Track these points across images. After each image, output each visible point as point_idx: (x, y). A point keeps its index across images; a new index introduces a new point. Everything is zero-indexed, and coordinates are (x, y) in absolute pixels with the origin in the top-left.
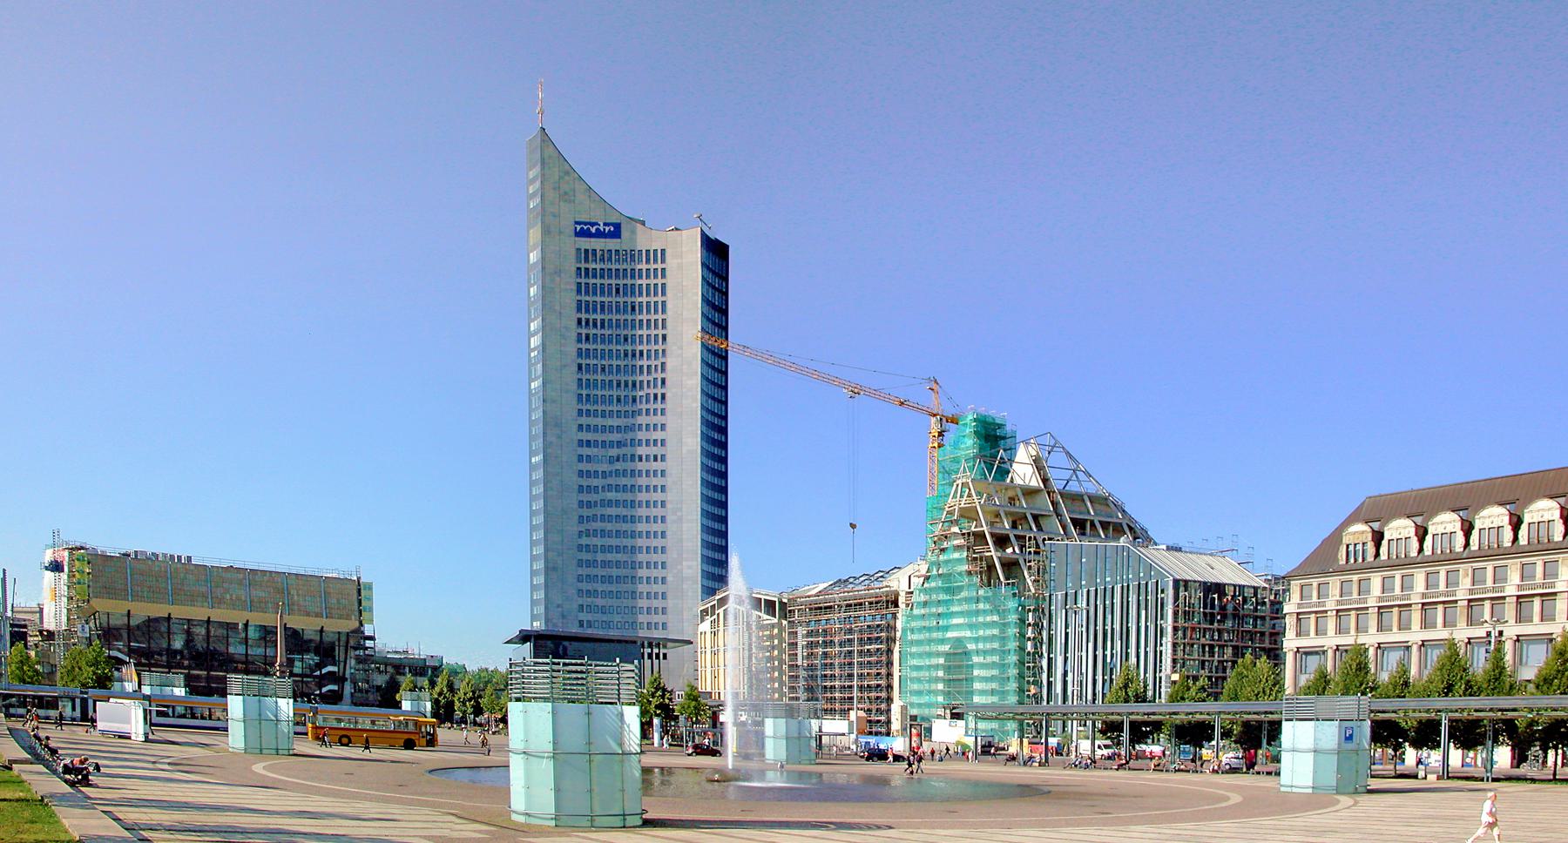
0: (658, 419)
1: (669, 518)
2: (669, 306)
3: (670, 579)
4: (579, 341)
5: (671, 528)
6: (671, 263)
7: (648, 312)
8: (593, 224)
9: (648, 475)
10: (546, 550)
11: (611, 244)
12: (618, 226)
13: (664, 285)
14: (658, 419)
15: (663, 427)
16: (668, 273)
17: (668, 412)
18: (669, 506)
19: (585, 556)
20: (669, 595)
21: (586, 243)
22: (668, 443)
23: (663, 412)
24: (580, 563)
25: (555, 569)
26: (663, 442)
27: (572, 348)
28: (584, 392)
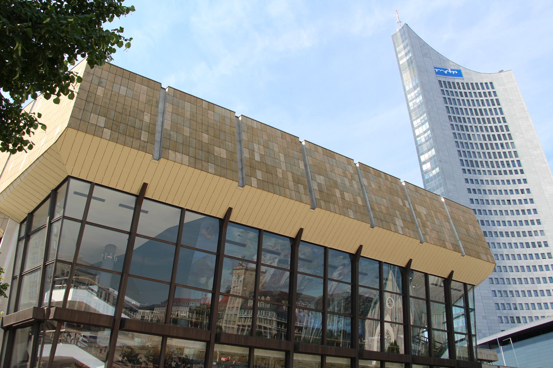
2: (504, 110)
8: (445, 70)
11: (457, 80)
12: (459, 71)
21: (442, 79)
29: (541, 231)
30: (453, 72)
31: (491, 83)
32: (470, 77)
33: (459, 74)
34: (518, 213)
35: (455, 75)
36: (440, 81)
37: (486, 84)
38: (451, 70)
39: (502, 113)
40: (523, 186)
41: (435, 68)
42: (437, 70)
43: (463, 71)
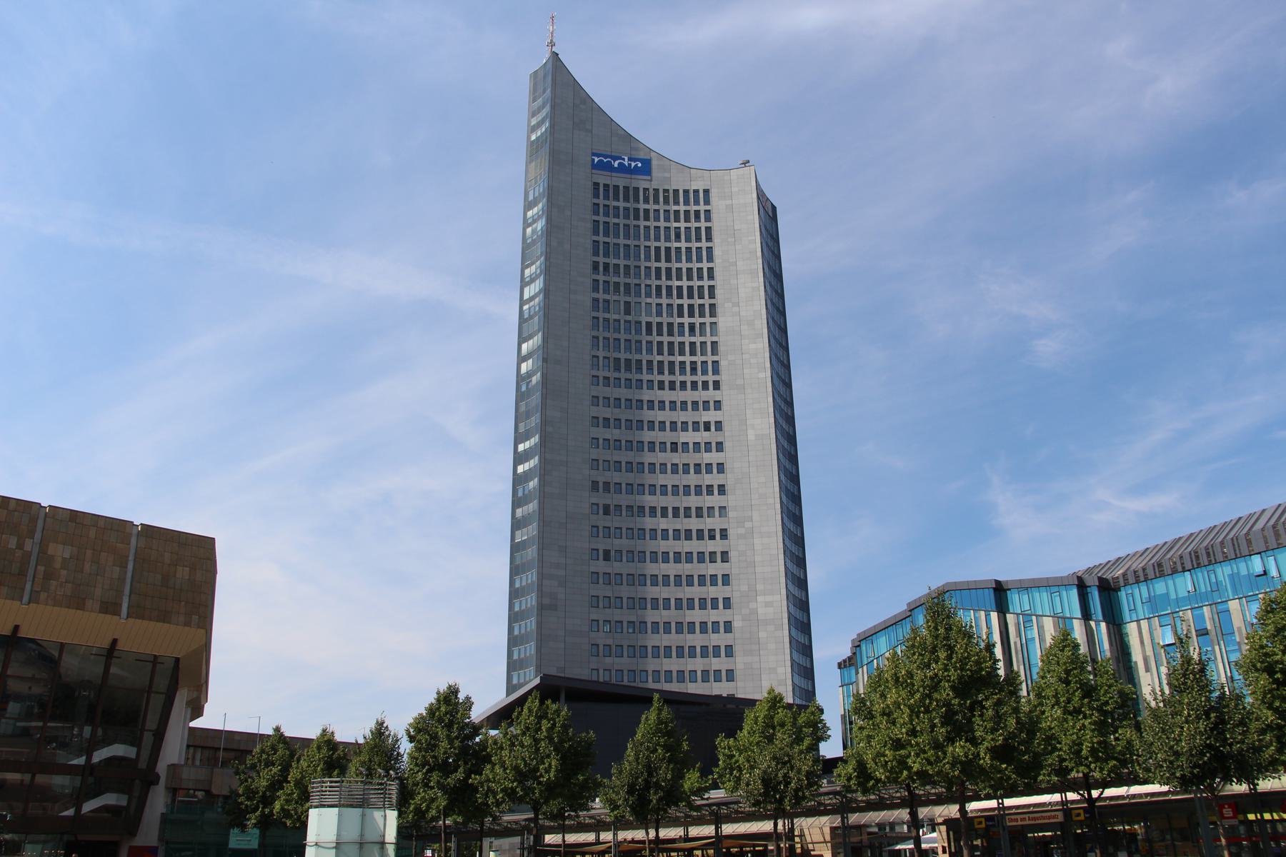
0: (711, 394)
1: (731, 533)
3: (737, 624)
4: (596, 289)
5: (735, 545)
6: (717, 204)
7: (689, 260)
9: (698, 471)
10: (541, 576)
12: (647, 164)
13: (708, 230)
14: (711, 394)
15: (718, 405)
16: (714, 216)
17: (723, 386)
18: (731, 514)
19: (602, 590)
20: (737, 649)
21: (603, 178)
22: (726, 426)
23: (717, 385)
24: (595, 601)
25: (553, 607)
26: (719, 425)
27: (586, 298)
28: (601, 354)
29: (722, 508)
30: (633, 164)
31: (706, 192)
32: (667, 175)
33: (646, 168)
34: (686, 471)
35: (636, 171)
36: (596, 185)
37: (696, 192)
38: (630, 159)
39: (710, 259)
40: (711, 416)
41: (594, 154)
42: (596, 160)
43: (654, 163)
